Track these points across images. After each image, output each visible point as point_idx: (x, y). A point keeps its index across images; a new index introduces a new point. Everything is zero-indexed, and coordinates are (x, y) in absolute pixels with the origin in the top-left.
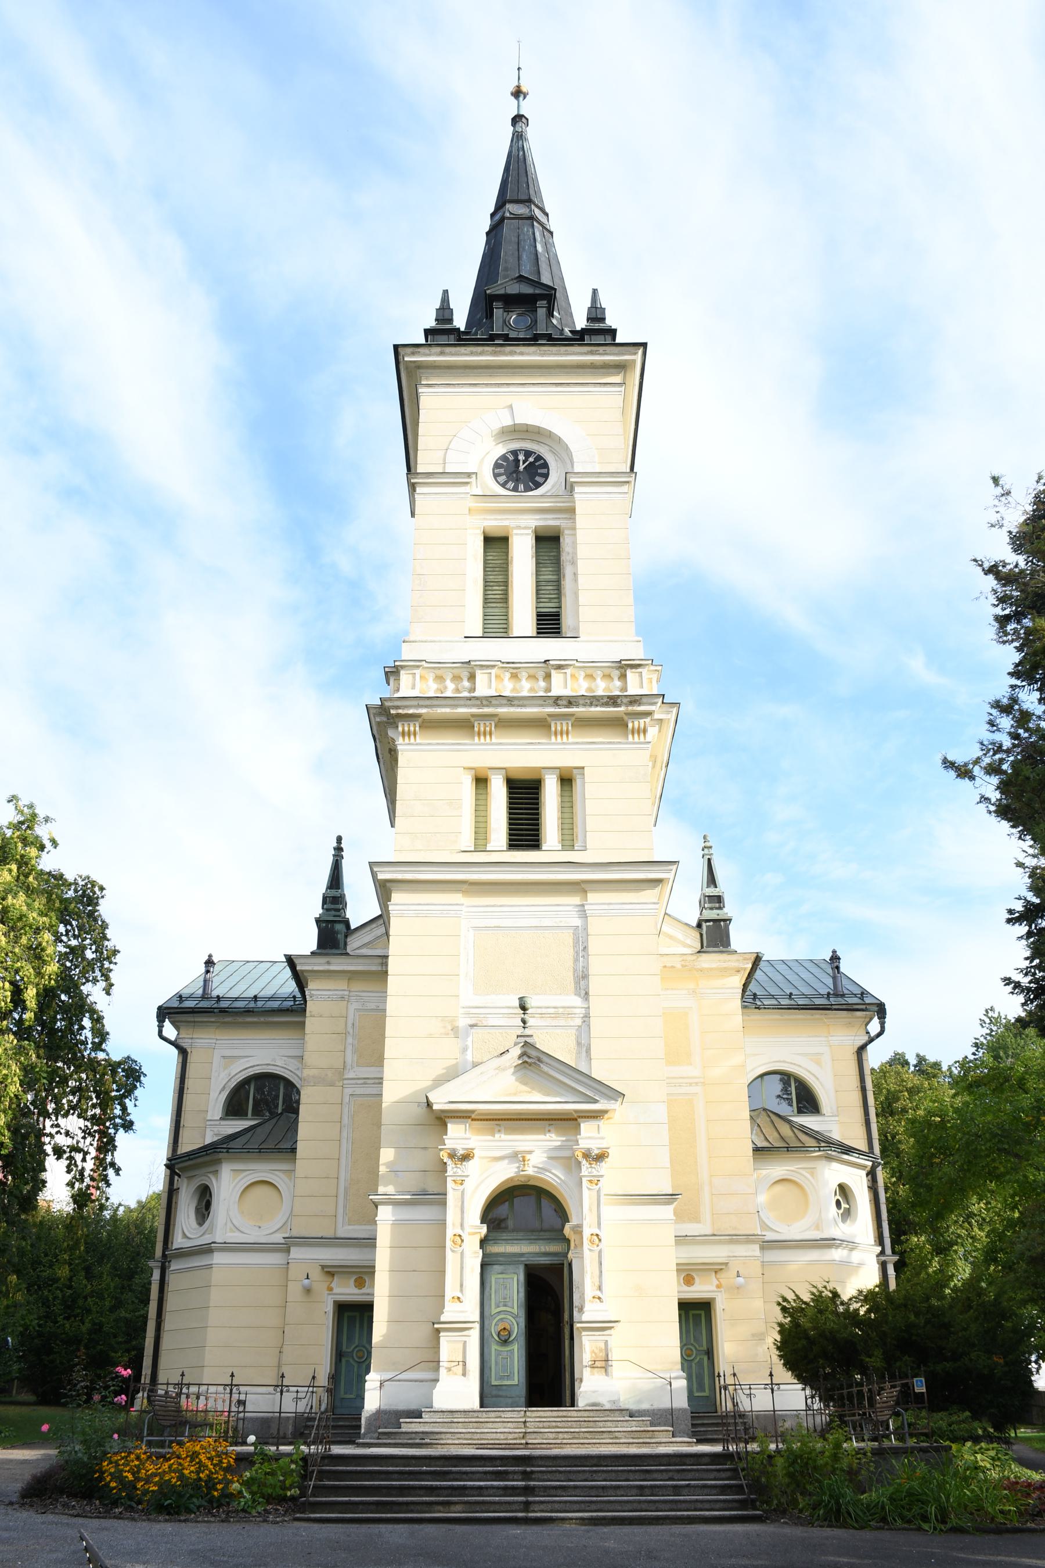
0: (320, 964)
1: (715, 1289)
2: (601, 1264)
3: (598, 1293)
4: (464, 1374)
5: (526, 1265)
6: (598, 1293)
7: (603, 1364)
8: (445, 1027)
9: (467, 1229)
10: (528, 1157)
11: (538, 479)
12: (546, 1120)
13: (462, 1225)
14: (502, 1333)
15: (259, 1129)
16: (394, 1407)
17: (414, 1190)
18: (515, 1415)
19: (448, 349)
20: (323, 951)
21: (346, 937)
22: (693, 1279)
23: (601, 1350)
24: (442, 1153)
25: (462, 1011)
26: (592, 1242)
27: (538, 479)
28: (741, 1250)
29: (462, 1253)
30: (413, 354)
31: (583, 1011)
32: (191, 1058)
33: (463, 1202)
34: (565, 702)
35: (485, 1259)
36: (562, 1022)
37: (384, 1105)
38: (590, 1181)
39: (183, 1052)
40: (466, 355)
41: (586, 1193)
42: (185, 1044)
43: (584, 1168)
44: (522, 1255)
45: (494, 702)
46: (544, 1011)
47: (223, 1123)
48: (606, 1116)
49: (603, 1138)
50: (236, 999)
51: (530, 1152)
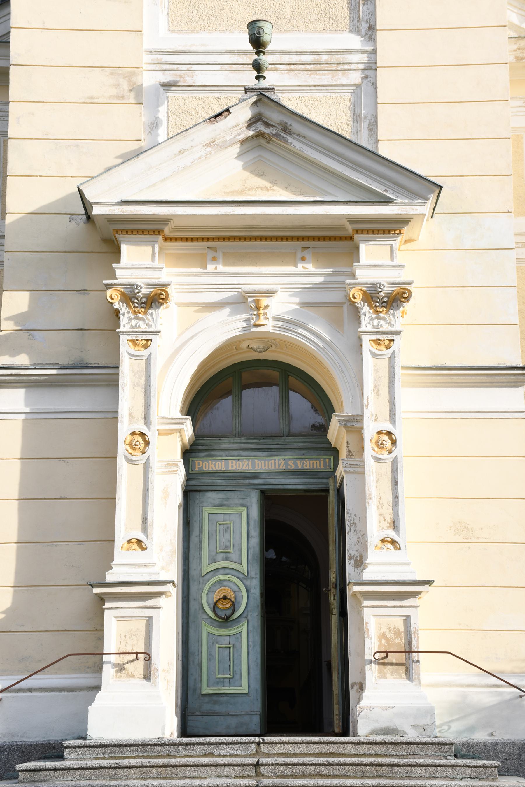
2: (395, 483)
3: (392, 534)
4: (147, 677)
5: (262, 492)
6: (392, 534)
7: (401, 658)
8: (117, 85)
9: (156, 424)
10: (264, 301)
12: (298, 239)
13: (146, 417)
14: (220, 606)
16: (18, 739)
17: (63, 361)
18: (240, 750)
23: (397, 634)
24: (109, 293)
25: (147, 58)
26: (380, 445)
29: (146, 465)
31: (364, 58)
33: (148, 378)
35: (192, 482)
36: (325, 79)
37: (9, 219)
38: (378, 342)
41: (368, 360)
43: (365, 320)
44: (255, 475)
46: (295, 58)
48: (406, 230)
49: (400, 267)
51: (270, 294)
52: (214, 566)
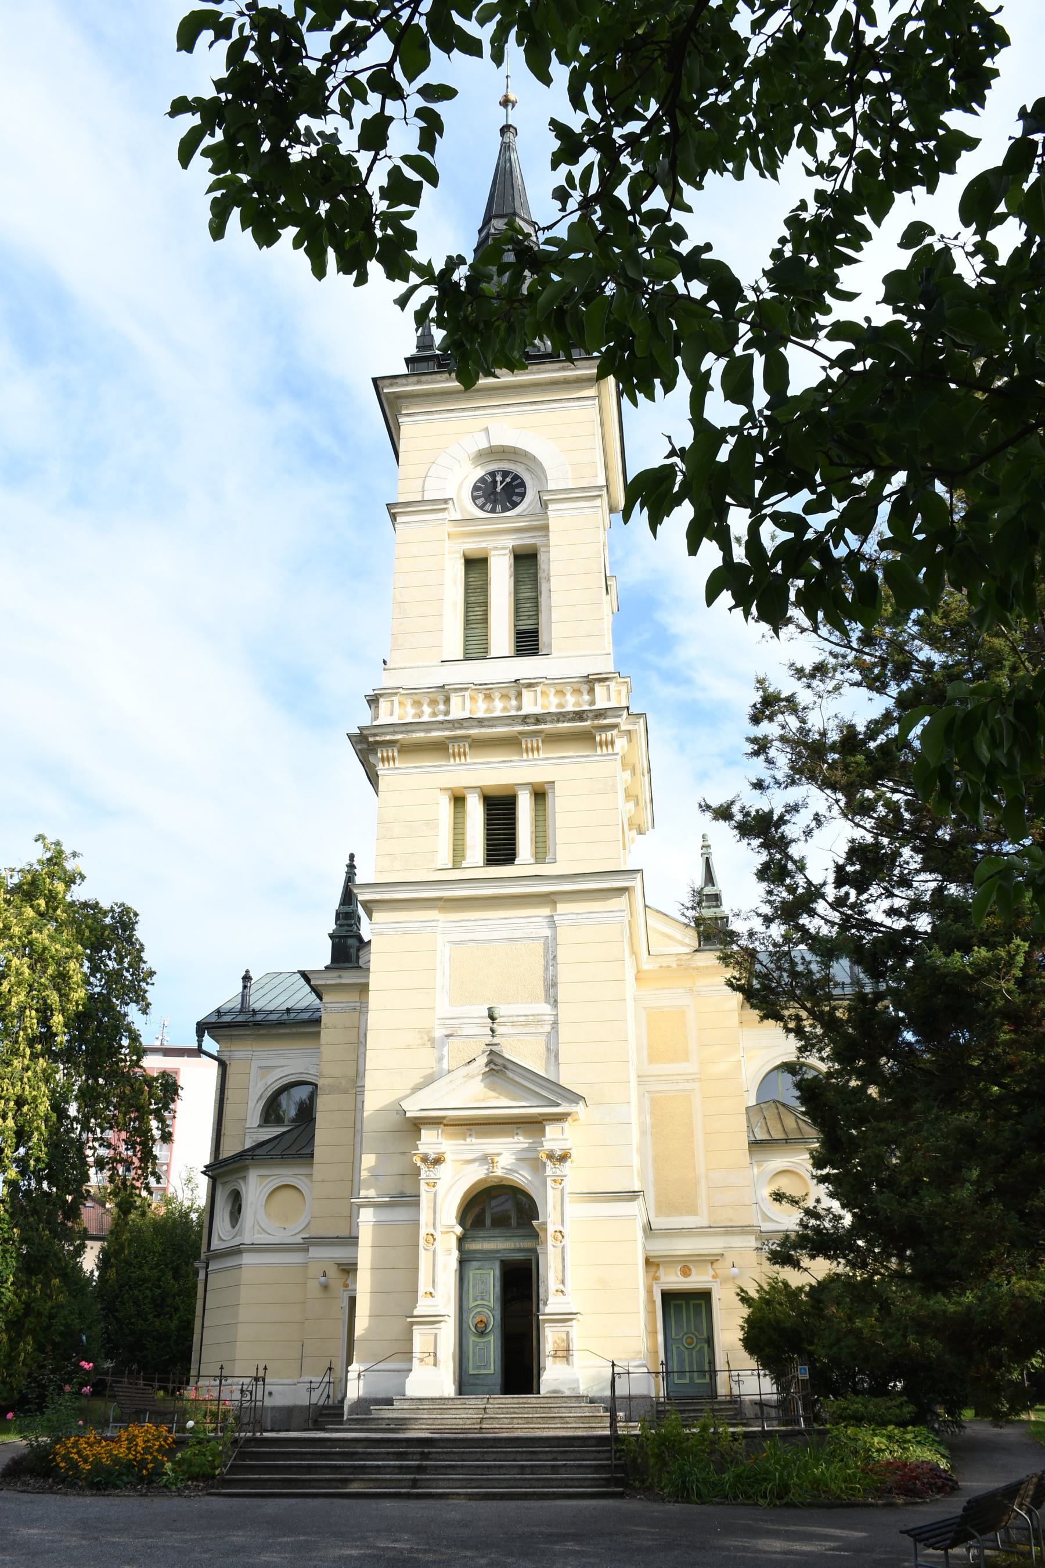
0: (332, 979)
1: (711, 1279)
2: (563, 1259)
3: (561, 1287)
4: (435, 1365)
5: (502, 1261)
6: (561, 1287)
7: (565, 1353)
8: (422, 1038)
9: (439, 1228)
10: (496, 1159)
11: (515, 498)
13: (434, 1225)
15: (287, 1136)
16: (373, 1396)
17: (393, 1192)
18: (479, 1402)
19: (424, 378)
20: (337, 966)
21: (358, 950)
22: (690, 1270)
23: (563, 1341)
24: (415, 1158)
25: (437, 1022)
26: (556, 1239)
27: (515, 498)
28: (737, 1241)
29: (434, 1252)
30: (391, 385)
31: (552, 1018)
32: (230, 1070)
33: (435, 1203)
34: (532, 720)
36: (532, 1030)
37: (365, 1114)
38: (555, 1181)
39: (223, 1065)
40: (442, 381)
41: (550, 1191)
42: (223, 1058)
43: (548, 1169)
44: (498, 1251)
45: (465, 724)
46: (515, 1019)
47: (261, 1130)
48: (569, 1119)
49: (566, 1140)
50: (271, 1012)
51: (499, 1155)
52: (476, 1303)
